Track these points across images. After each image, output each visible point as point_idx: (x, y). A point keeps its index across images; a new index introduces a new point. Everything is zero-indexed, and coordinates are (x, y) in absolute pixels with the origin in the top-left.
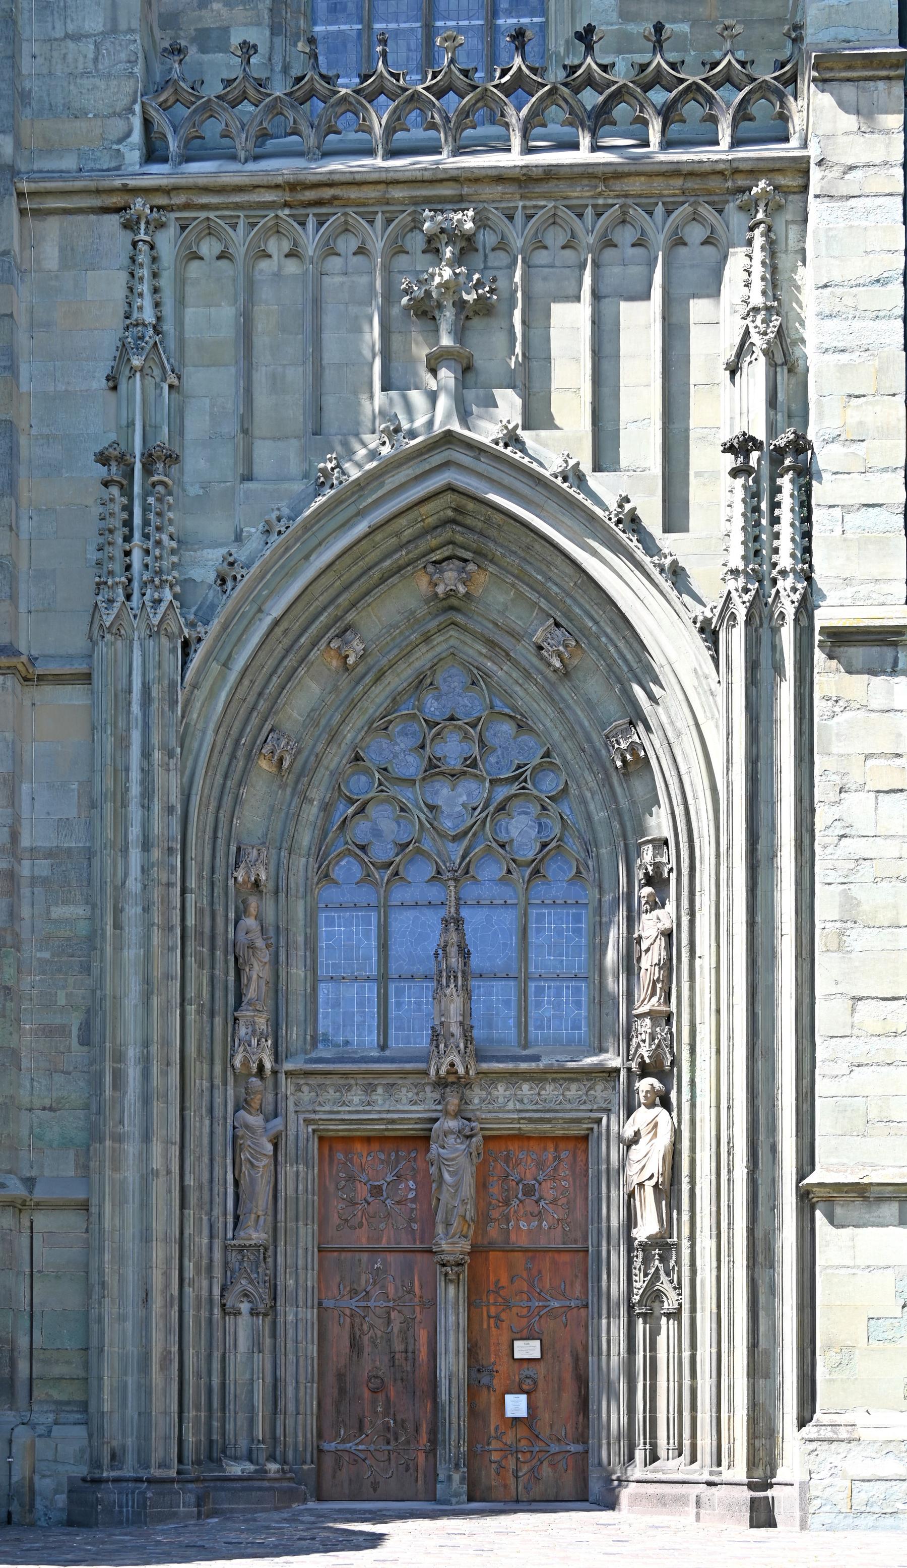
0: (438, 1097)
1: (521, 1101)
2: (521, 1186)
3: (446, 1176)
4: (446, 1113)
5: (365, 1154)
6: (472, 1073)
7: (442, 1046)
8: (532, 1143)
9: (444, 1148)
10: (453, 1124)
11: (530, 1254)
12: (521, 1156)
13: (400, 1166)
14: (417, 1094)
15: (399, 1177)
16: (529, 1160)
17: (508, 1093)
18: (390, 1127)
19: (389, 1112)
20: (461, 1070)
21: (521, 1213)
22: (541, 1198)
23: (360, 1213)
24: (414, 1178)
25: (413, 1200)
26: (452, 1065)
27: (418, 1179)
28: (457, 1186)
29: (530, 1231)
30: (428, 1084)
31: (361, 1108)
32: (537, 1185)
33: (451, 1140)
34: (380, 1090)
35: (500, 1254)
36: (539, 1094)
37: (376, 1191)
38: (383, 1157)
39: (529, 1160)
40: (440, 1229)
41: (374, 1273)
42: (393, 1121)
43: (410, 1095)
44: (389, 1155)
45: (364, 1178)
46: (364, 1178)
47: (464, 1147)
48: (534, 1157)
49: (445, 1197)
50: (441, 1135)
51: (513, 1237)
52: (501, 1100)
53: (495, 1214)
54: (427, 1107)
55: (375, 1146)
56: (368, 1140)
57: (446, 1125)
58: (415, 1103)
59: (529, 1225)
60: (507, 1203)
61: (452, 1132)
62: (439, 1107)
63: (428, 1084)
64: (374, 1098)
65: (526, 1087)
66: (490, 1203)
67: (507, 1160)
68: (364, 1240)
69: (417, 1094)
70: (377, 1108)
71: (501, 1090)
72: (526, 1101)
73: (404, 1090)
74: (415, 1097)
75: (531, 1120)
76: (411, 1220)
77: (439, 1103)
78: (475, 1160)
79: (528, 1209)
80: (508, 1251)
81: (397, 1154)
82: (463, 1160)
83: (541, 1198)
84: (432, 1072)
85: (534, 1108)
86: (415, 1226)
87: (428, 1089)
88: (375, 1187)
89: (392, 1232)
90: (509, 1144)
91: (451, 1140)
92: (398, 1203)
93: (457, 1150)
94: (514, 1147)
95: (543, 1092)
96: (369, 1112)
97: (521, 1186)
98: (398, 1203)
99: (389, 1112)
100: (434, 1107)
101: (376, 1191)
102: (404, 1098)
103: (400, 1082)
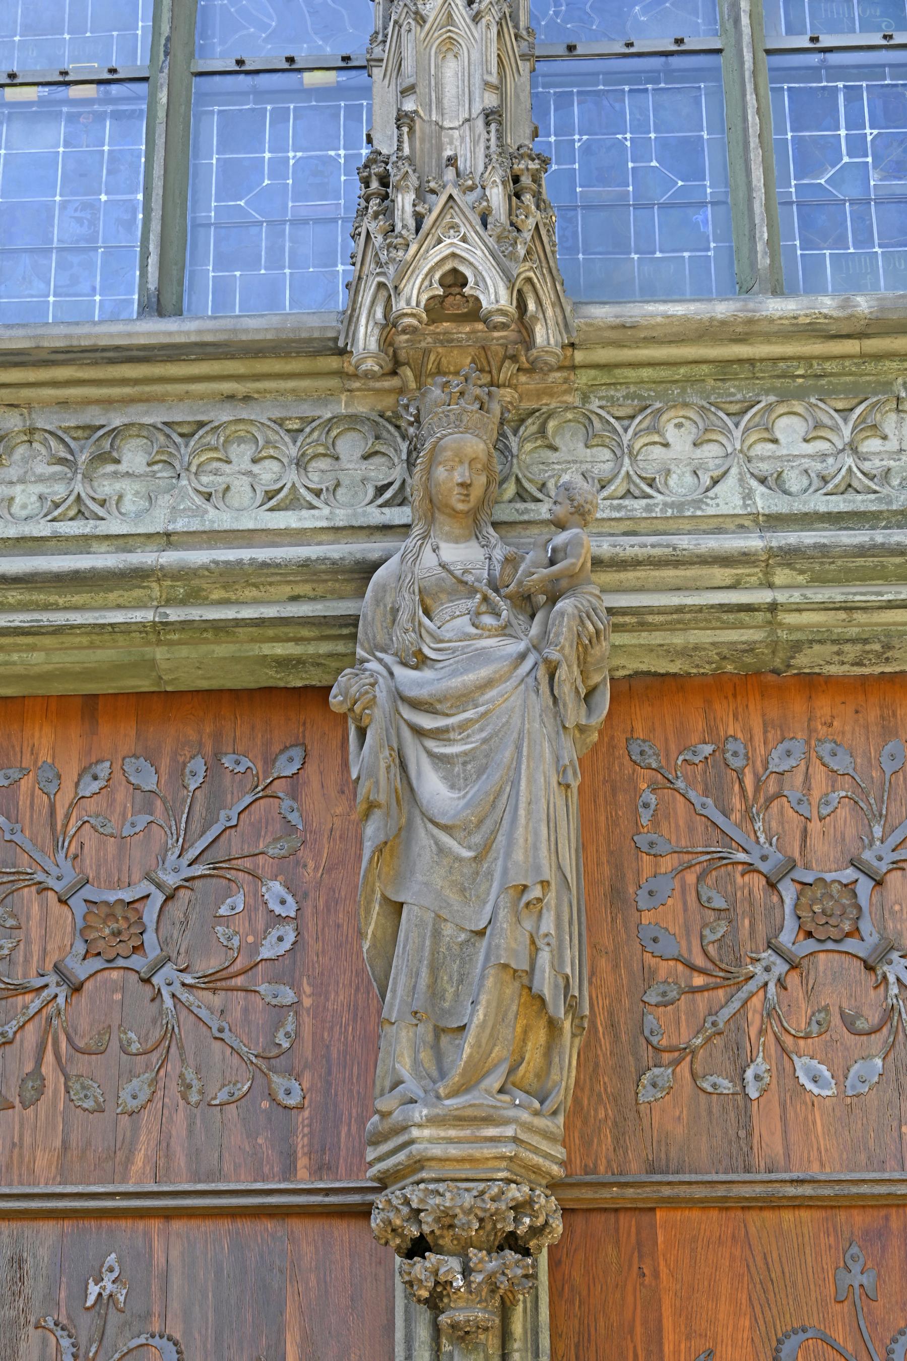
0: (397, 473)
1: (773, 482)
2: (788, 891)
3: (433, 786)
4: (433, 507)
5: (70, 774)
6: (545, 335)
7: (404, 202)
8: (824, 706)
9: (421, 661)
10: (461, 554)
11: (859, 1219)
12: (778, 764)
13: (227, 816)
14: (301, 463)
15: (220, 867)
16: (819, 775)
17: (710, 451)
18: (174, 615)
19: (168, 539)
20: (494, 295)
21: (798, 1022)
22: (886, 949)
23: (31, 1034)
24: (288, 868)
25: (286, 969)
26: (455, 280)
27: (309, 875)
28: (485, 827)
29: (849, 1106)
30: (352, 421)
31: (43, 529)
32: (864, 886)
33: (455, 620)
34: (134, 457)
35: (710, 1222)
36: (853, 448)
37: (115, 930)
38: (150, 782)
39: (819, 775)
40: (403, 1052)
41: (86, 1324)
42: (189, 585)
43: (268, 473)
44: (179, 772)
45: (60, 872)
46: (60, 872)
47: (515, 647)
48: (840, 763)
49: (426, 886)
50: (408, 603)
51: (769, 1137)
52: (680, 484)
53: (672, 1027)
54: (342, 517)
55: (119, 736)
56: (89, 708)
57: (428, 559)
58: (293, 503)
59: (841, 1075)
60: (729, 976)
61: (462, 586)
62: (398, 515)
63: (352, 421)
64: (107, 488)
65: (790, 429)
66: (649, 975)
67: (718, 776)
68: (42, 1161)
69: (301, 463)
70: (115, 526)
71: (677, 449)
72: (794, 481)
73: (241, 454)
74: (292, 476)
75: (817, 564)
76: (271, 1059)
77: (400, 499)
78: (574, 714)
79: (831, 997)
80: (747, 1205)
81: (214, 768)
82: (514, 703)
83: (886, 949)
84: (366, 338)
85: (838, 504)
86: (290, 1090)
87: (350, 446)
88: (110, 910)
89: (180, 1118)
90: (722, 709)
91: (455, 620)
92: (212, 982)
93: (482, 657)
94: (744, 728)
95: (872, 445)
96: (84, 543)
97: (788, 891)
98: (212, 982)
99: (168, 539)
100: (377, 516)
101: (115, 930)
102: (241, 485)
103: (224, 415)
